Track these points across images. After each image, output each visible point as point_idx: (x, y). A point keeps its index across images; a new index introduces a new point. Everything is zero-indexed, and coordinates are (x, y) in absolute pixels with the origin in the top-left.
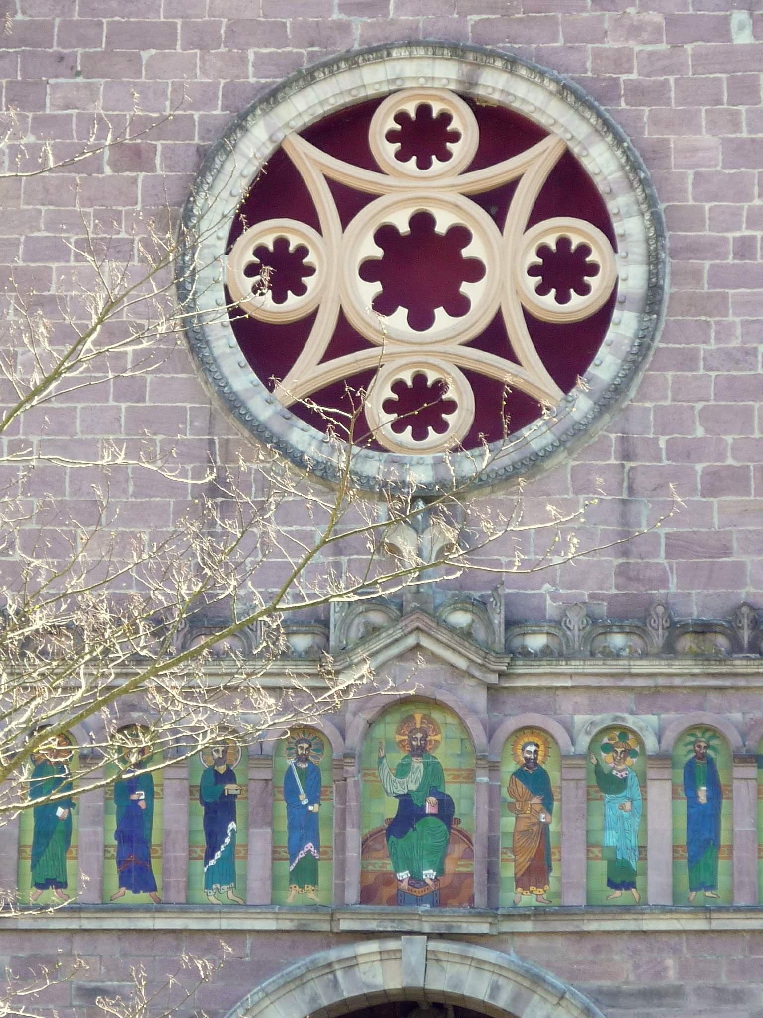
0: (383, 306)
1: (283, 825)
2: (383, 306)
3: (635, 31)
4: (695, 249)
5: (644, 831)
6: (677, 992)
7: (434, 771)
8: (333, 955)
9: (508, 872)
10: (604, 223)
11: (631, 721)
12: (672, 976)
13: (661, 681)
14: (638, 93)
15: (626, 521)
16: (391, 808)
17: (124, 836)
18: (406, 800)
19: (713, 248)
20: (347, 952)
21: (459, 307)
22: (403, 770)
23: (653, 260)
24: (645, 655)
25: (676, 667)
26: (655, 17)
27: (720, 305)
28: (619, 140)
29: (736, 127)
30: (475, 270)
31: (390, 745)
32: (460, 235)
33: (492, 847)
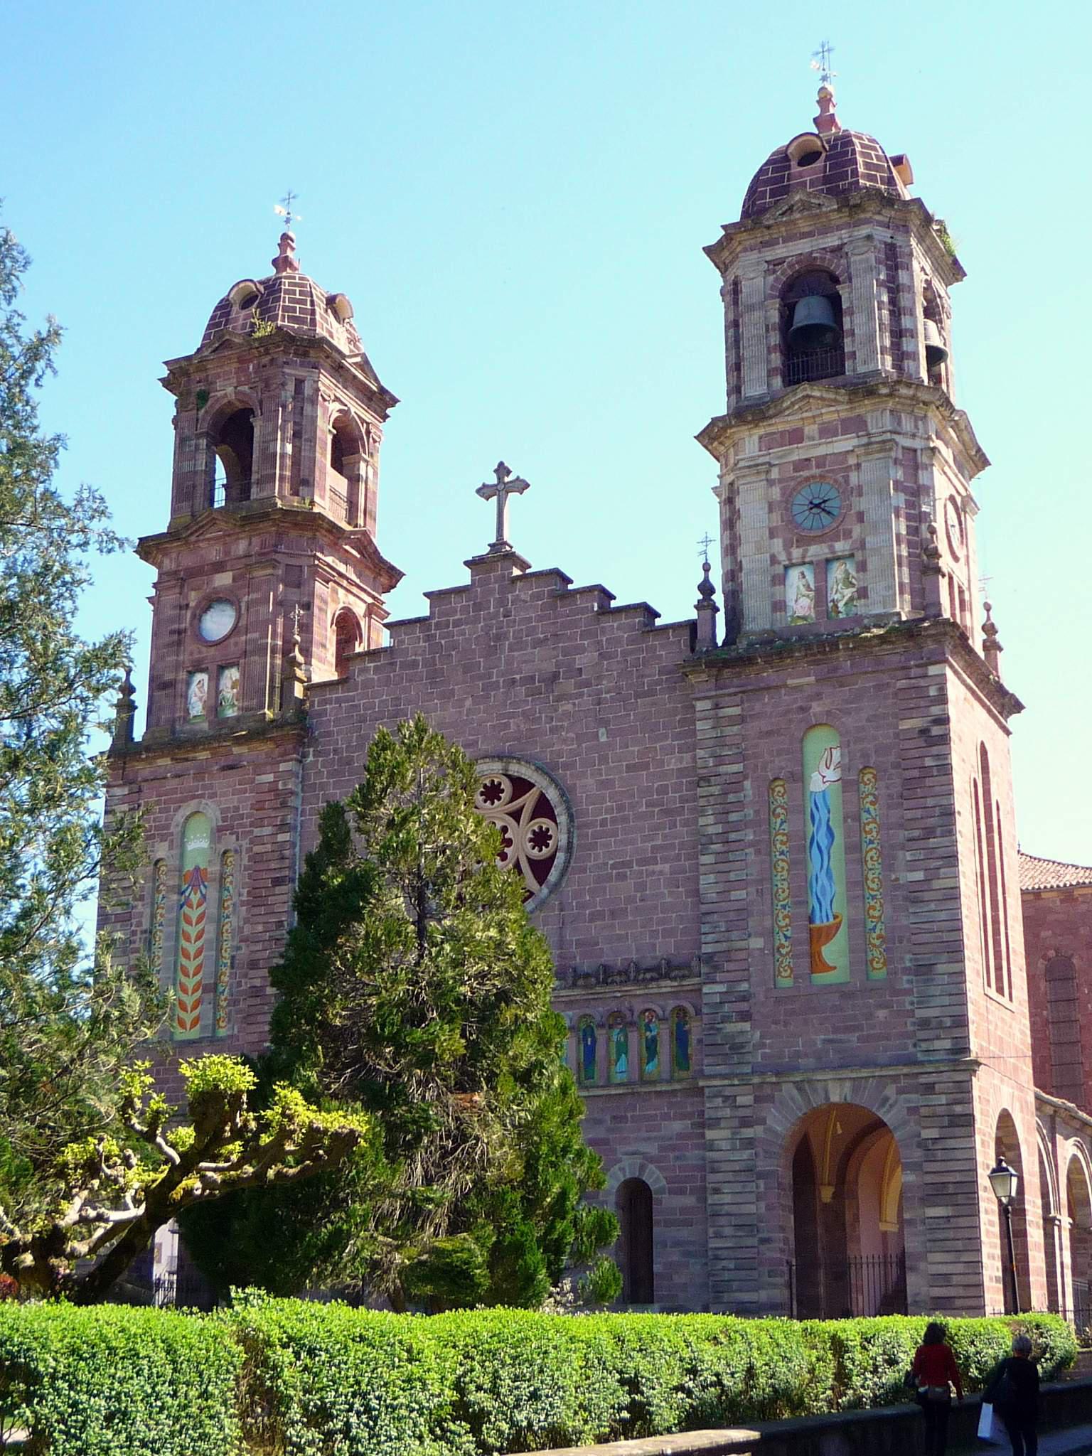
3: (564, 741)
4: (586, 825)
13: (572, 998)
14: (566, 766)
15: (561, 936)
19: (592, 824)
23: (569, 832)
24: (565, 988)
25: (576, 992)
26: (572, 735)
27: (593, 846)
28: (557, 786)
29: (601, 775)
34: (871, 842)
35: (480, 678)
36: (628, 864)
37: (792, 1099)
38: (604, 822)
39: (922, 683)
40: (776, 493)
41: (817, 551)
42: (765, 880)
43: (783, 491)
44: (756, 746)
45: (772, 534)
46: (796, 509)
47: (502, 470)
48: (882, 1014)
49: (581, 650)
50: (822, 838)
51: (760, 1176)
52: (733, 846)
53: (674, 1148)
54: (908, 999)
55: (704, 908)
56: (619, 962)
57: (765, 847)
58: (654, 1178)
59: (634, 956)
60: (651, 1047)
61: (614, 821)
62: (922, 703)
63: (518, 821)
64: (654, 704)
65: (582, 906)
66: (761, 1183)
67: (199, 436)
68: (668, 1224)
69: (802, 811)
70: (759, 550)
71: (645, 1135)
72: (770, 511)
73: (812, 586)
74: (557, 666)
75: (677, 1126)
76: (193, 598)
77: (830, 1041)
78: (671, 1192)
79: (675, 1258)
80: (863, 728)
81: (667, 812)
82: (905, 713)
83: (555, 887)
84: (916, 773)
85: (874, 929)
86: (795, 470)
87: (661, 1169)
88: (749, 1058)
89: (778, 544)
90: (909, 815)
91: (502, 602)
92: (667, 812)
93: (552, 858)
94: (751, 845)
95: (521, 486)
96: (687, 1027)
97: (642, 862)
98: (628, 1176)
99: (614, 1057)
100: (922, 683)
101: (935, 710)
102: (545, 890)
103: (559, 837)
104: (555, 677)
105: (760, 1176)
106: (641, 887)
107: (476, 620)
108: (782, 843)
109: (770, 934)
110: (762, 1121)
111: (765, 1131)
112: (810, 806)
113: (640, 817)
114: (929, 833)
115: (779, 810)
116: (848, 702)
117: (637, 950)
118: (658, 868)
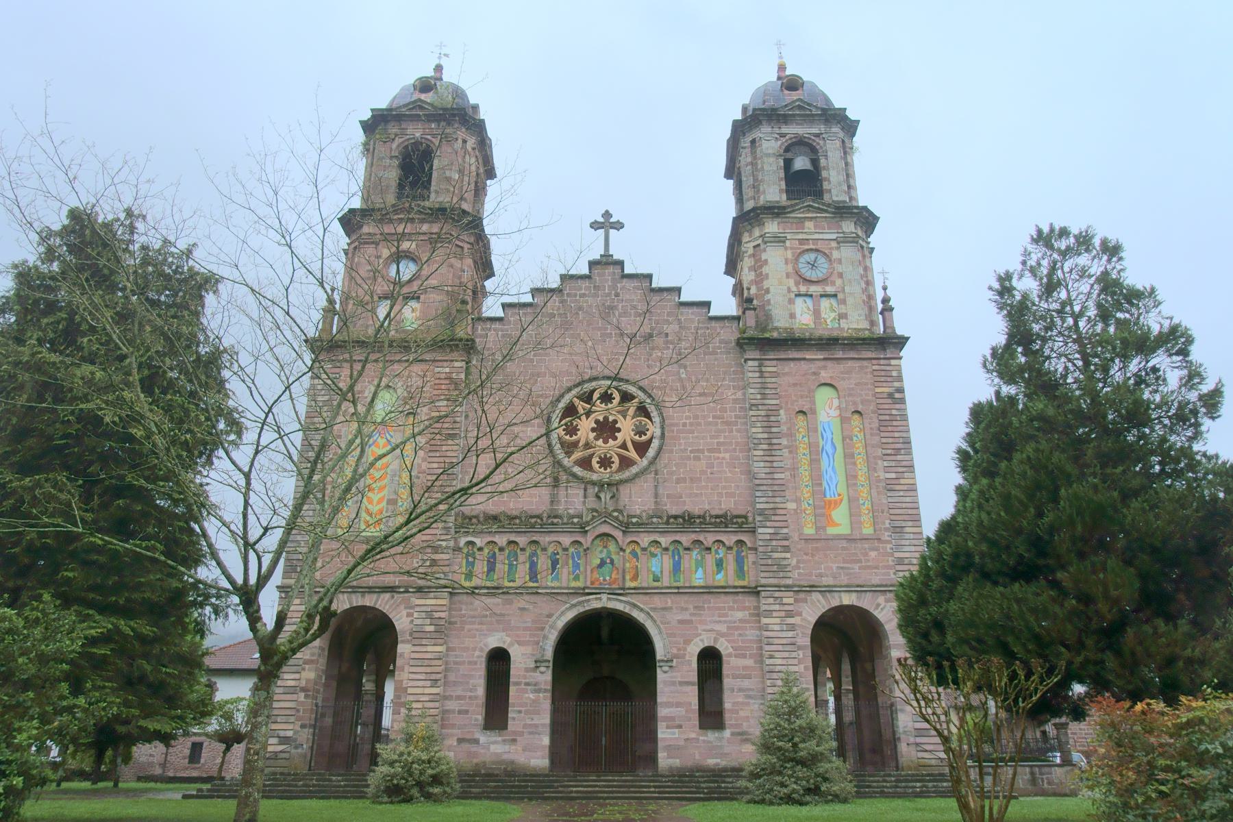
0: (596, 439)
1: (571, 566)
2: (596, 439)
5: (662, 567)
6: (671, 608)
7: (609, 552)
8: (584, 598)
9: (628, 577)
10: (650, 418)
11: (658, 539)
12: (669, 604)
14: (659, 388)
16: (598, 561)
17: (531, 568)
18: (602, 559)
19: (677, 425)
20: (588, 597)
21: (615, 439)
22: (601, 552)
23: (662, 428)
30: (619, 430)
31: (598, 546)
32: (615, 422)
33: (624, 571)
34: (859, 454)
35: (599, 329)
36: (702, 451)
37: (818, 601)
38: (684, 425)
39: (888, 368)
40: (789, 254)
41: (813, 289)
42: (794, 469)
43: (793, 254)
44: (786, 391)
45: (788, 276)
46: (800, 265)
47: (607, 215)
48: (873, 554)
49: (670, 323)
50: (829, 448)
51: (800, 648)
52: (775, 447)
53: (737, 628)
54: (889, 546)
55: (757, 482)
56: (696, 511)
57: (793, 450)
58: (723, 647)
59: (707, 507)
60: (719, 564)
61: (691, 424)
62: (889, 379)
63: (625, 418)
64: (716, 359)
65: (672, 473)
66: (801, 653)
67: (391, 157)
68: (735, 677)
69: (816, 431)
70: (780, 283)
71: (718, 619)
72: (786, 263)
73: (811, 308)
74: (652, 329)
75: (740, 615)
76: (386, 253)
77: (842, 568)
78: (736, 657)
79: (740, 700)
80: (853, 389)
81: (727, 423)
82: (876, 383)
83: (653, 462)
84: (887, 418)
85: (864, 504)
86: (800, 244)
87: (729, 641)
88: (789, 574)
89: (791, 282)
90: (884, 440)
91: (614, 287)
92: (727, 423)
93: (650, 441)
94: (786, 447)
95: (619, 226)
96: (743, 554)
97: (710, 451)
98: (706, 645)
99: (694, 569)
100: (888, 368)
101: (897, 384)
102: (644, 462)
103: (654, 429)
104: (651, 336)
105: (800, 648)
106: (711, 466)
107: (596, 295)
108: (804, 449)
109: (798, 501)
110: (800, 614)
111: (802, 620)
112: (820, 429)
113: (710, 424)
114: (897, 451)
115: (801, 430)
116: (842, 373)
117: (709, 504)
118: (721, 455)
